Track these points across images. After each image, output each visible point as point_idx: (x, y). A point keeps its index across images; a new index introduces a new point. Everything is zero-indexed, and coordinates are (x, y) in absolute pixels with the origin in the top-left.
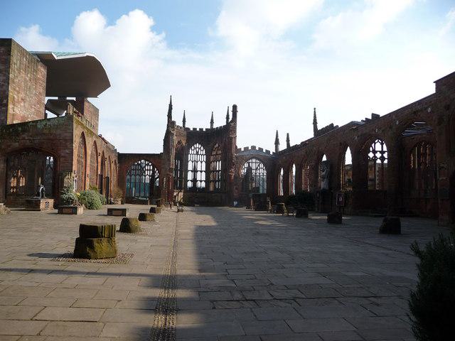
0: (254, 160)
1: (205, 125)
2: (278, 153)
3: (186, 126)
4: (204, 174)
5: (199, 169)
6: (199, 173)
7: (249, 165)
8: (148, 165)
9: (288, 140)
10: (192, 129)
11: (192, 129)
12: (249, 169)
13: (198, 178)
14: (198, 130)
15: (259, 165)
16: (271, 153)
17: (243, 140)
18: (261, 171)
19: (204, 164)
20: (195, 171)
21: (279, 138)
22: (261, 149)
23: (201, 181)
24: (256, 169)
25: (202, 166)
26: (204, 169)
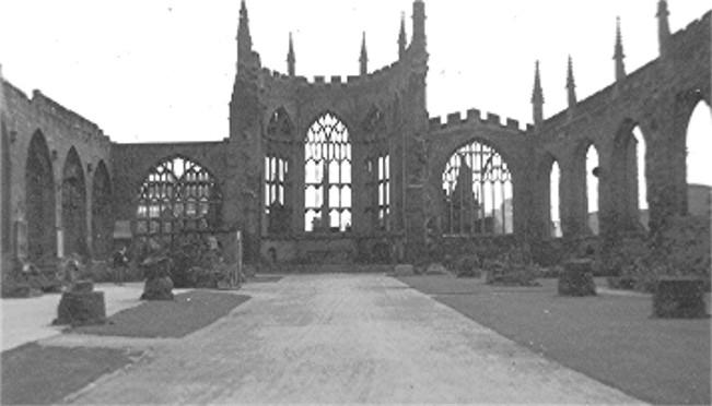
0: (476, 147)
1: (348, 69)
2: (544, 128)
3: (298, 73)
4: (347, 192)
5: (333, 179)
7: (463, 159)
9: (571, 85)
10: (311, 80)
11: (311, 80)
12: (466, 172)
13: (333, 203)
14: (328, 80)
15: (490, 160)
16: (523, 127)
17: (442, 100)
19: (347, 167)
21: (543, 85)
22: (494, 118)
23: (340, 210)
24: (484, 170)
25: (343, 172)
26: (347, 178)
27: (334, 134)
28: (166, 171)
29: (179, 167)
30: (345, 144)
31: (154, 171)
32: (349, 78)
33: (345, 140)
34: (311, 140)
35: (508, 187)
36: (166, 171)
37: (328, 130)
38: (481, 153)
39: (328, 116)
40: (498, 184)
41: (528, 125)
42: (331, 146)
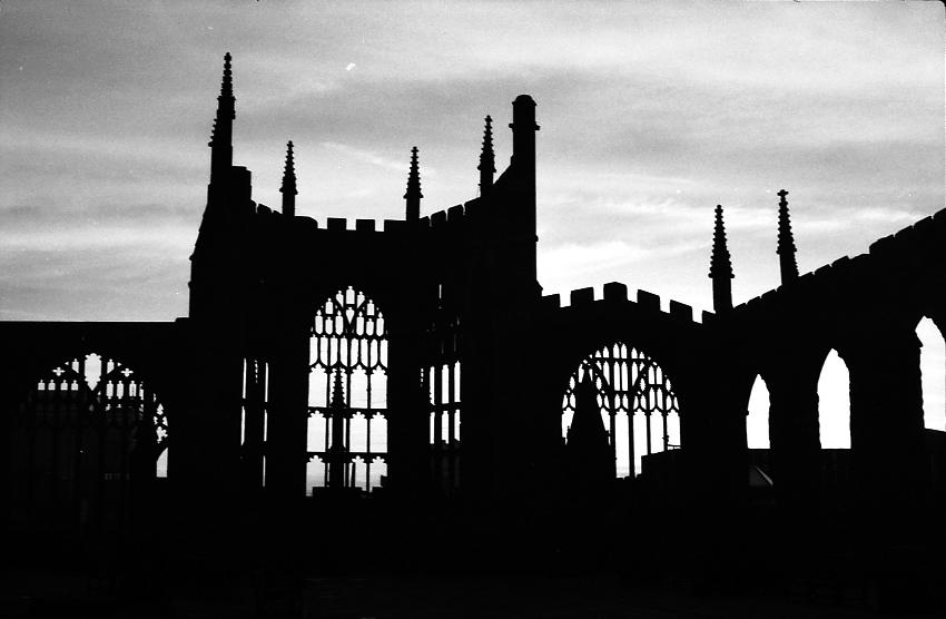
0: (620, 351)
4: (380, 423)
5: (358, 400)
6: (358, 422)
7: (600, 373)
8: (116, 376)
9: (786, 247)
10: (323, 225)
13: (357, 445)
14: (351, 226)
15: (643, 374)
16: (697, 318)
18: (656, 398)
19: (380, 378)
20: (339, 410)
22: (649, 300)
23: (368, 457)
24: (633, 391)
25: (370, 389)
26: (380, 401)
27: (360, 321)
28: (70, 376)
29: (93, 367)
30: (379, 339)
31: (48, 377)
32: (388, 223)
33: (380, 332)
34: (319, 331)
35: (674, 420)
36: (70, 376)
37: (350, 313)
38: (629, 361)
39: (350, 292)
40: (656, 417)
41: (705, 314)
42: (355, 342)
